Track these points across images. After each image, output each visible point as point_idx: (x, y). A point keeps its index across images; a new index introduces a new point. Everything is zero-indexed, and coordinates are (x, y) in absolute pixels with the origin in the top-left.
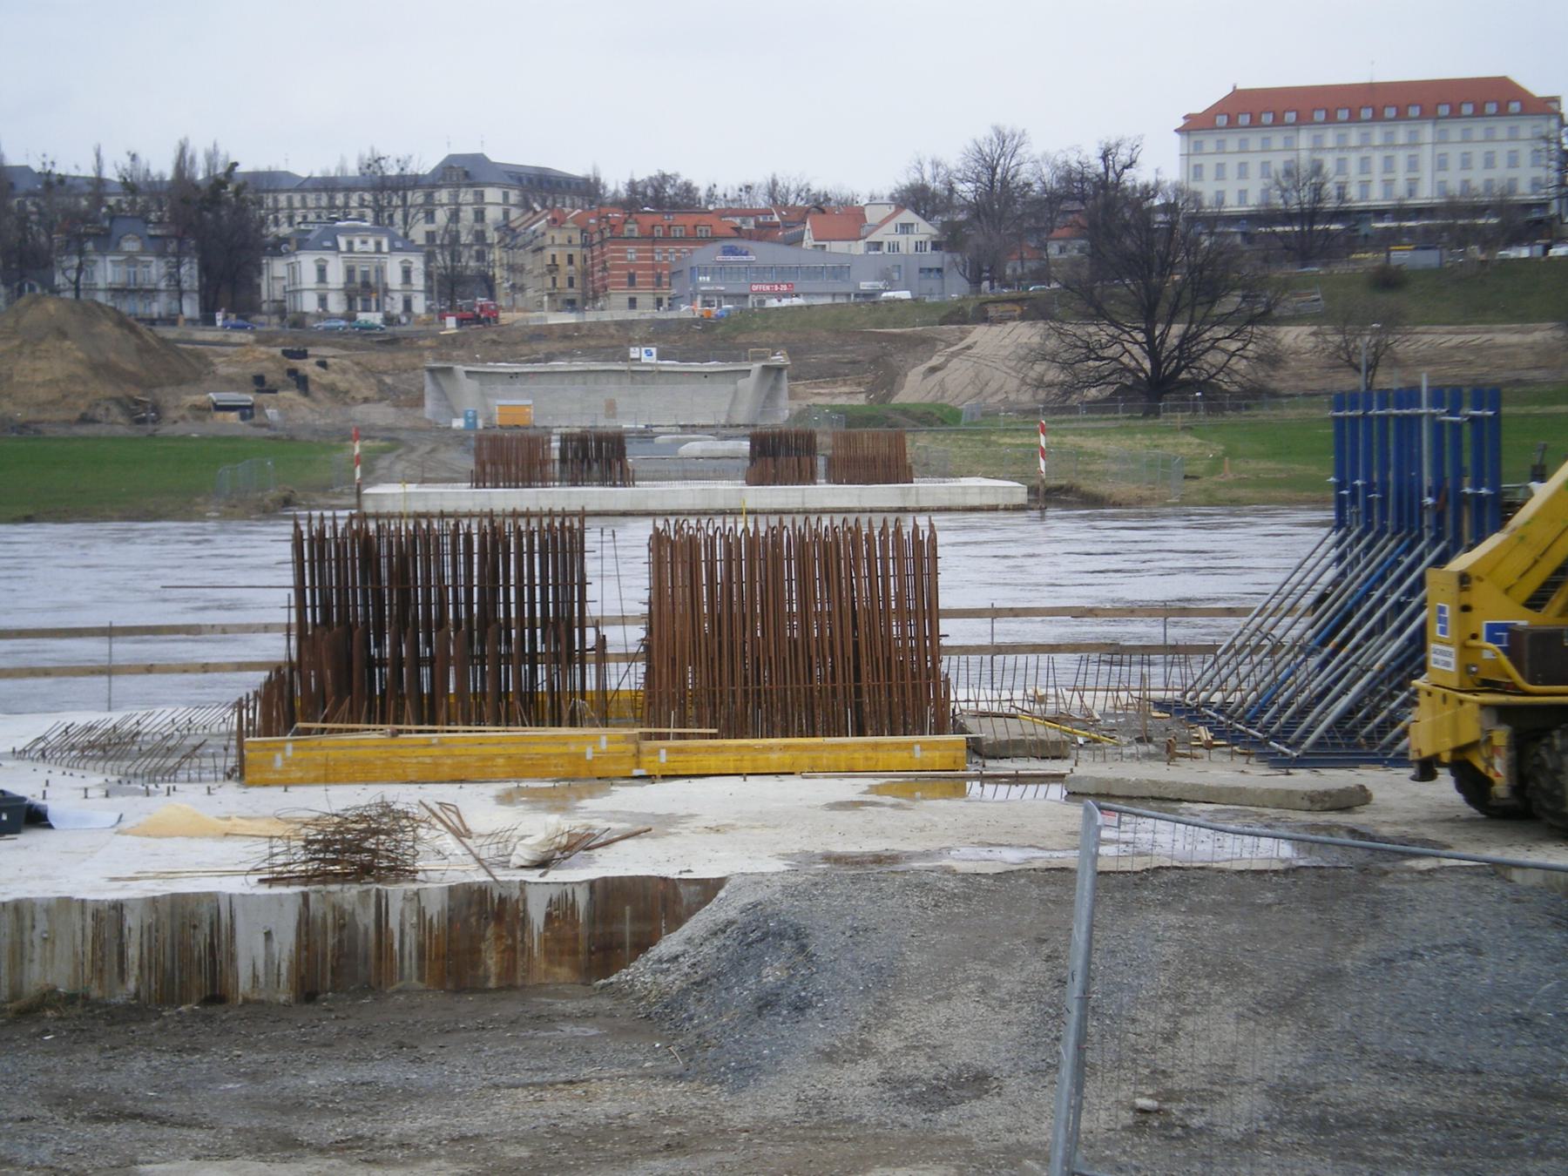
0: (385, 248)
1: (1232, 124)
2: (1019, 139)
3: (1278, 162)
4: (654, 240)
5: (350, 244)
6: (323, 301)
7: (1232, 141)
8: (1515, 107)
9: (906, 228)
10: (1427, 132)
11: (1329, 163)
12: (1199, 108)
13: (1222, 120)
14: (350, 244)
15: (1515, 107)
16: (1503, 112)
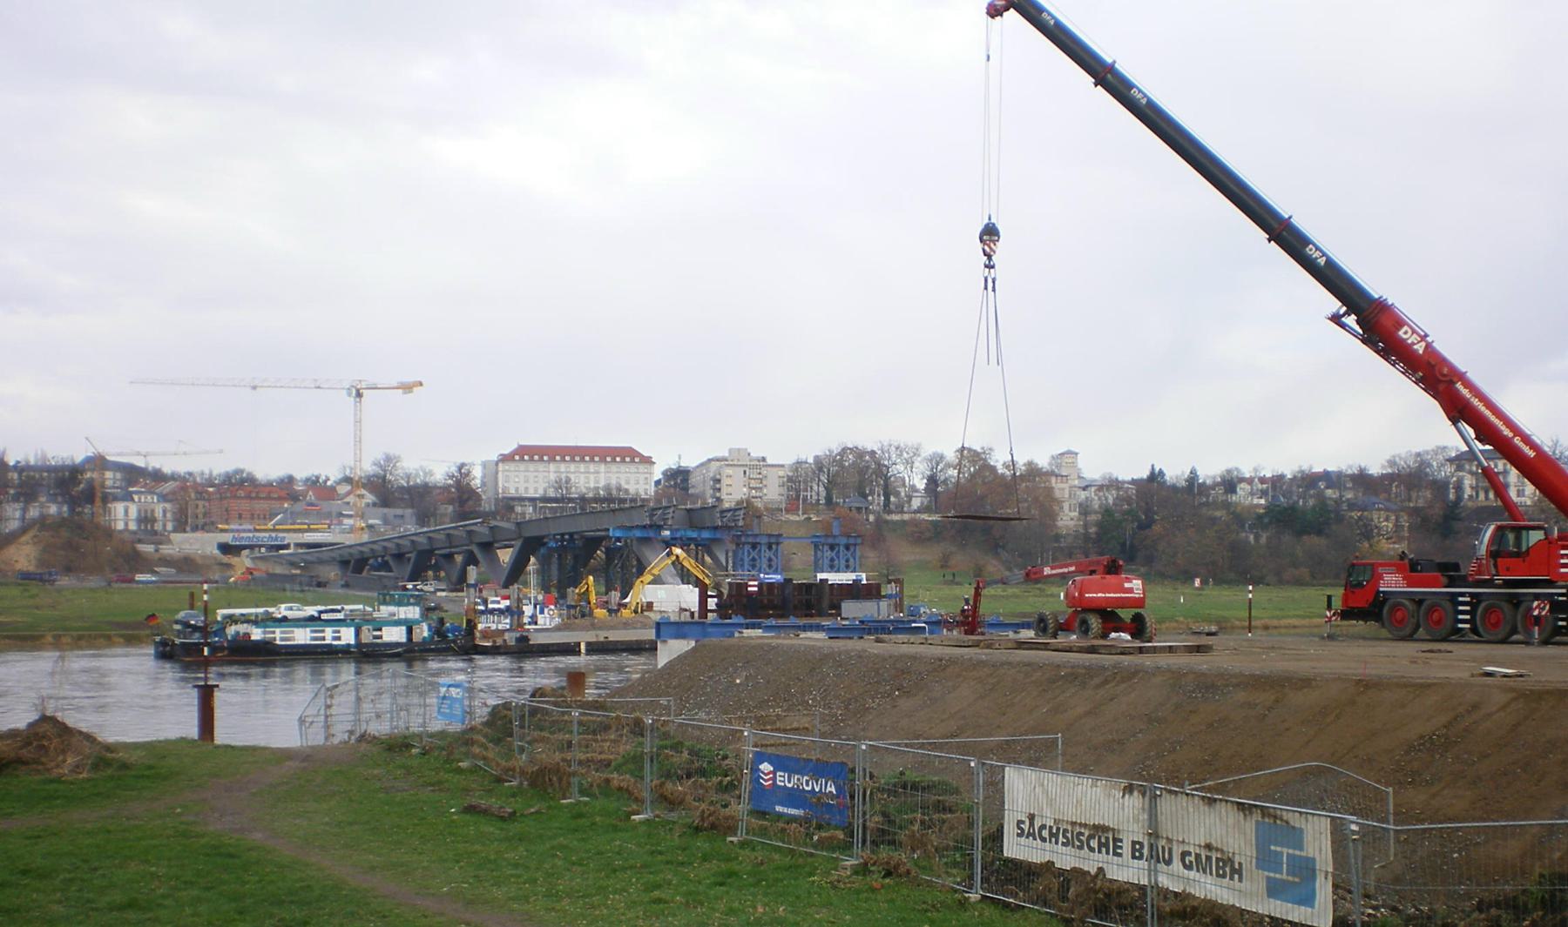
0: (155, 500)
1: (522, 459)
2: (398, 459)
3: (553, 477)
4: (251, 498)
5: (140, 499)
6: (126, 524)
7: (522, 466)
8: (637, 460)
9: (361, 496)
10: (602, 467)
11: (572, 477)
12: (507, 451)
13: (517, 458)
14: (140, 499)
15: (637, 460)
16: (633, 461)
